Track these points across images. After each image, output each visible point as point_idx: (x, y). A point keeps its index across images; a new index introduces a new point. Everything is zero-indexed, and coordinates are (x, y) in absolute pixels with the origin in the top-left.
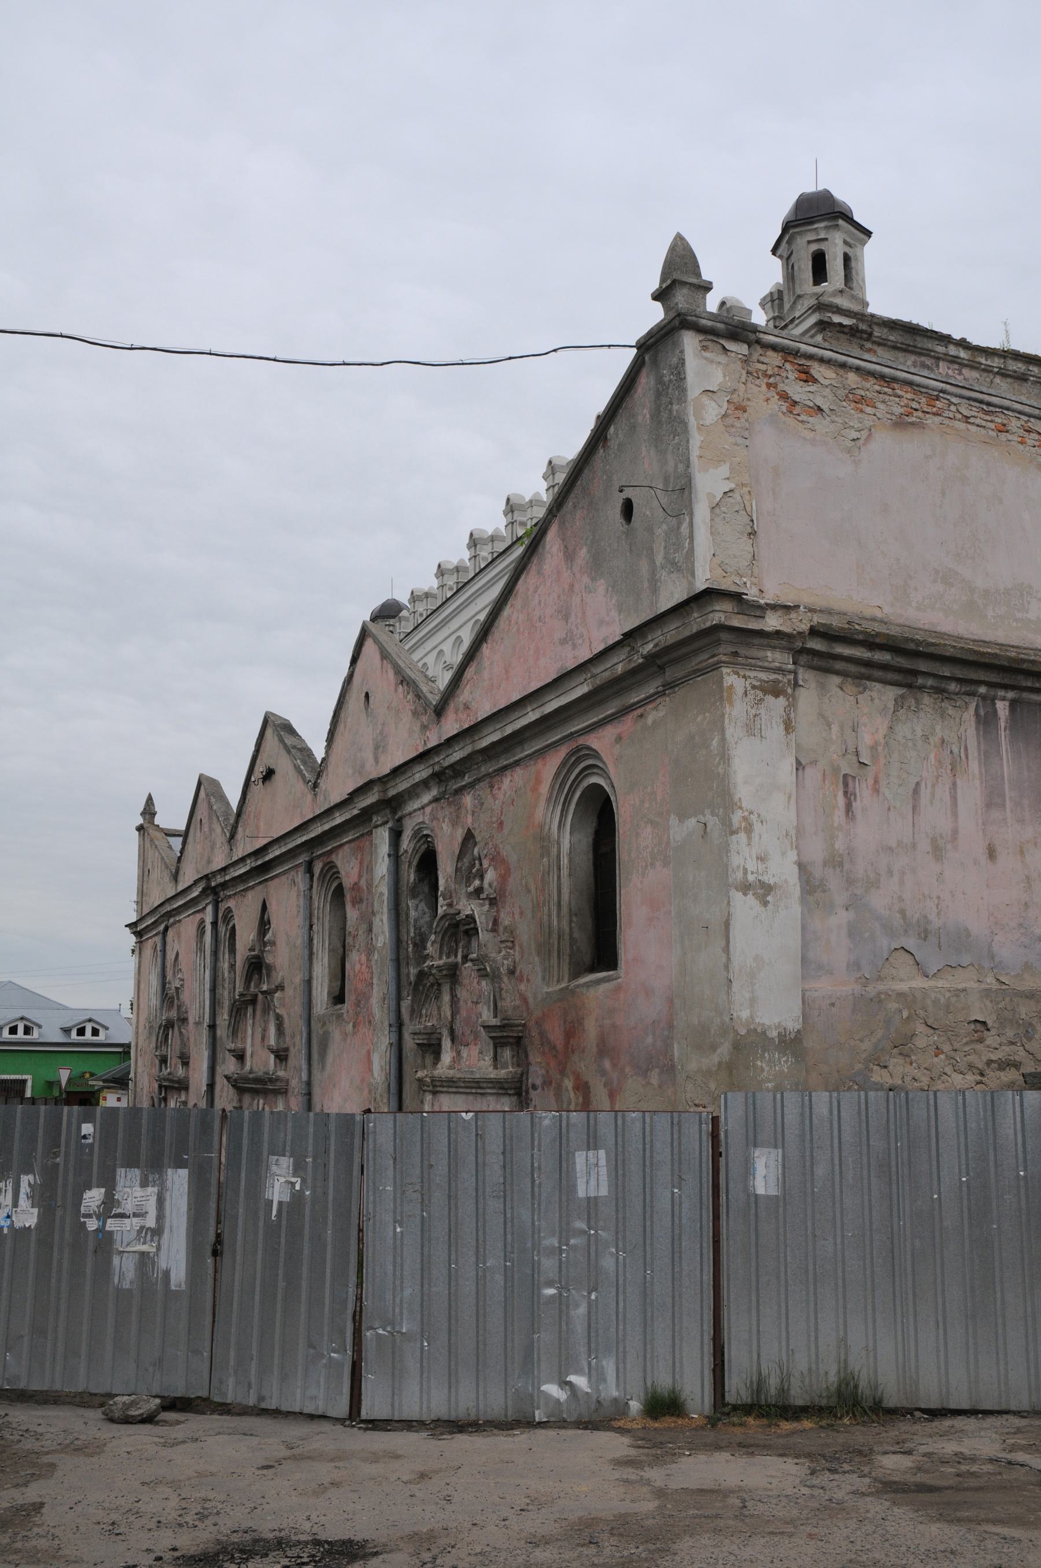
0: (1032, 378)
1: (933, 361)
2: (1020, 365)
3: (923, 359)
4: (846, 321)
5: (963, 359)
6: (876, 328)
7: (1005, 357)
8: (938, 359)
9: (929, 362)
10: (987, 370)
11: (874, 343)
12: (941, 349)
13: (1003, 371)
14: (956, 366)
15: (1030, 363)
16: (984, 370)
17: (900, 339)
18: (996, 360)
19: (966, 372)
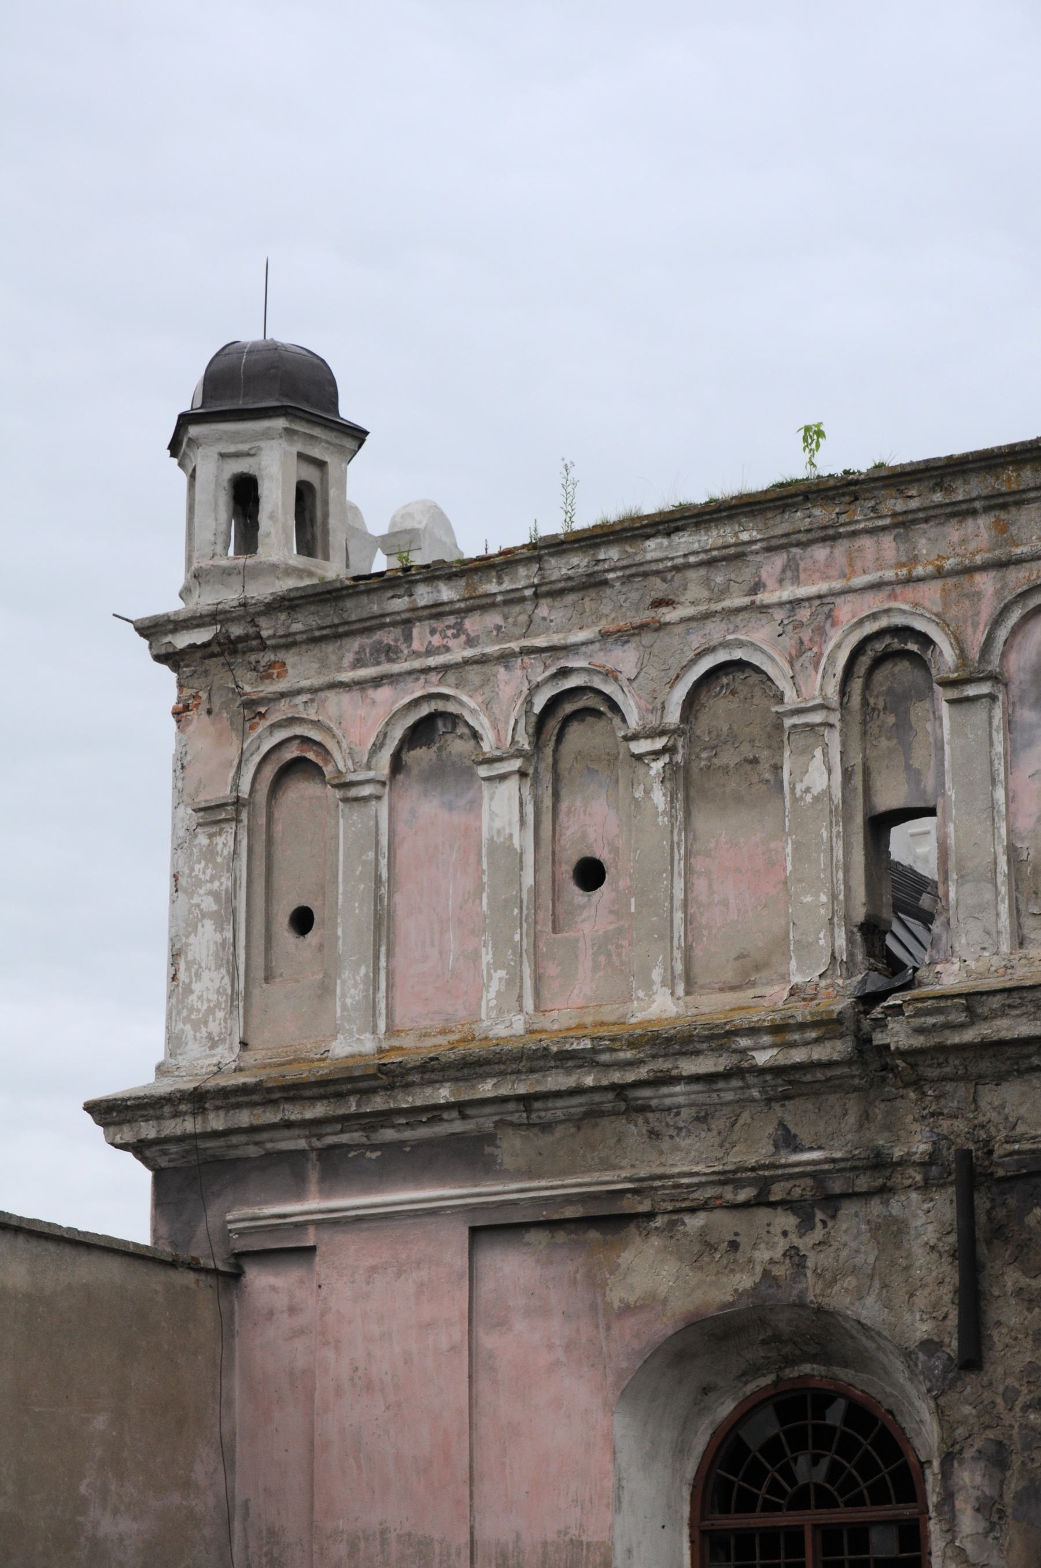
0: (611, 576)
1: (398, 631)
2: (575, 560)
3: (378, 635)
4: (201, 636)
5: (451, 602)
6: (263, 622)
7: (539, 559)
8: (408, 622)
9: (387, 637)
10: (513, 599)
11: (276, 648)
12: (399, 604)
13: (544, 589)
14: (451, 620)
15: (597, 546)
16: (506, 603)
17: (313, 621)
18: (522, 571)
19: (473, 624)
